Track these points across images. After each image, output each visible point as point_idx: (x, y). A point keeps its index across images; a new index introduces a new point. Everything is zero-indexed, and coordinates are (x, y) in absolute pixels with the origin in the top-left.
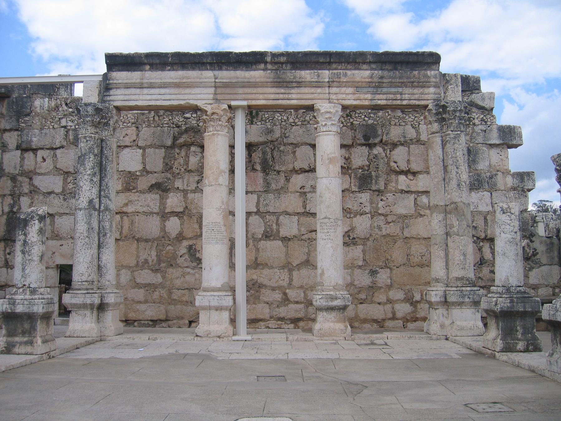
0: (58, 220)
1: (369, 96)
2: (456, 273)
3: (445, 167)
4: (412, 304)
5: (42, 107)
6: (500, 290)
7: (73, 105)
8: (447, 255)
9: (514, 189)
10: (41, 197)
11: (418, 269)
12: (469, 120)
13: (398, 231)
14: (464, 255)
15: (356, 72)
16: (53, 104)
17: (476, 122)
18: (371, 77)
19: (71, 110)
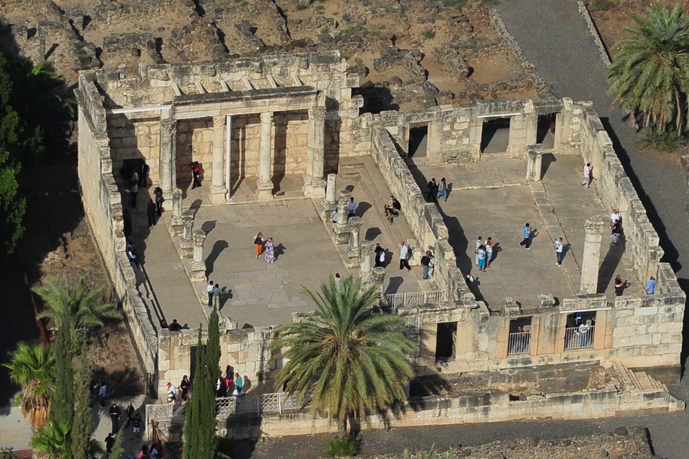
0: (124, 139)
1: (285, 108)
2: (316, 175)
3: (315, 135)
4: (297, 163)
5: (113, 87)
6: (327, 203)
7: (129, 83)
8: (313, 167)
9: (352, 108)
10: (115, 130)
11: (301, 148)
12: (332, 77)
13: (292, 131)
14: (320, 169)
15: (280, 99)
16: (119, 85)
17: (336, 78)
18: (287, 101)
19: (128, 86)
